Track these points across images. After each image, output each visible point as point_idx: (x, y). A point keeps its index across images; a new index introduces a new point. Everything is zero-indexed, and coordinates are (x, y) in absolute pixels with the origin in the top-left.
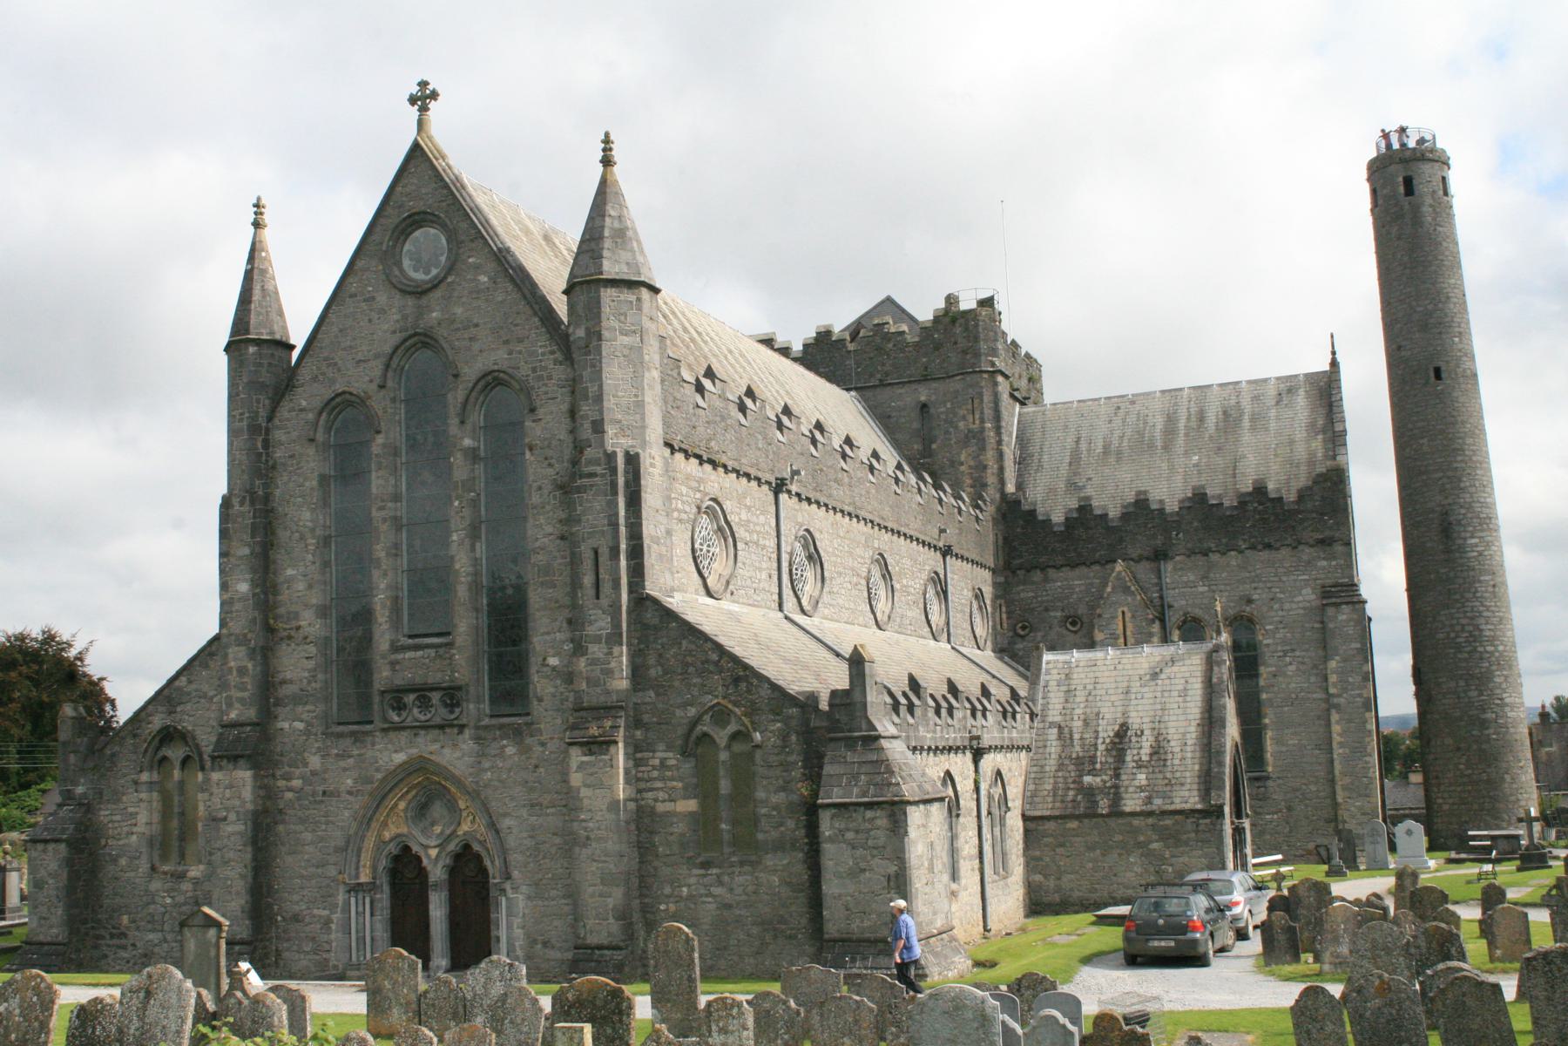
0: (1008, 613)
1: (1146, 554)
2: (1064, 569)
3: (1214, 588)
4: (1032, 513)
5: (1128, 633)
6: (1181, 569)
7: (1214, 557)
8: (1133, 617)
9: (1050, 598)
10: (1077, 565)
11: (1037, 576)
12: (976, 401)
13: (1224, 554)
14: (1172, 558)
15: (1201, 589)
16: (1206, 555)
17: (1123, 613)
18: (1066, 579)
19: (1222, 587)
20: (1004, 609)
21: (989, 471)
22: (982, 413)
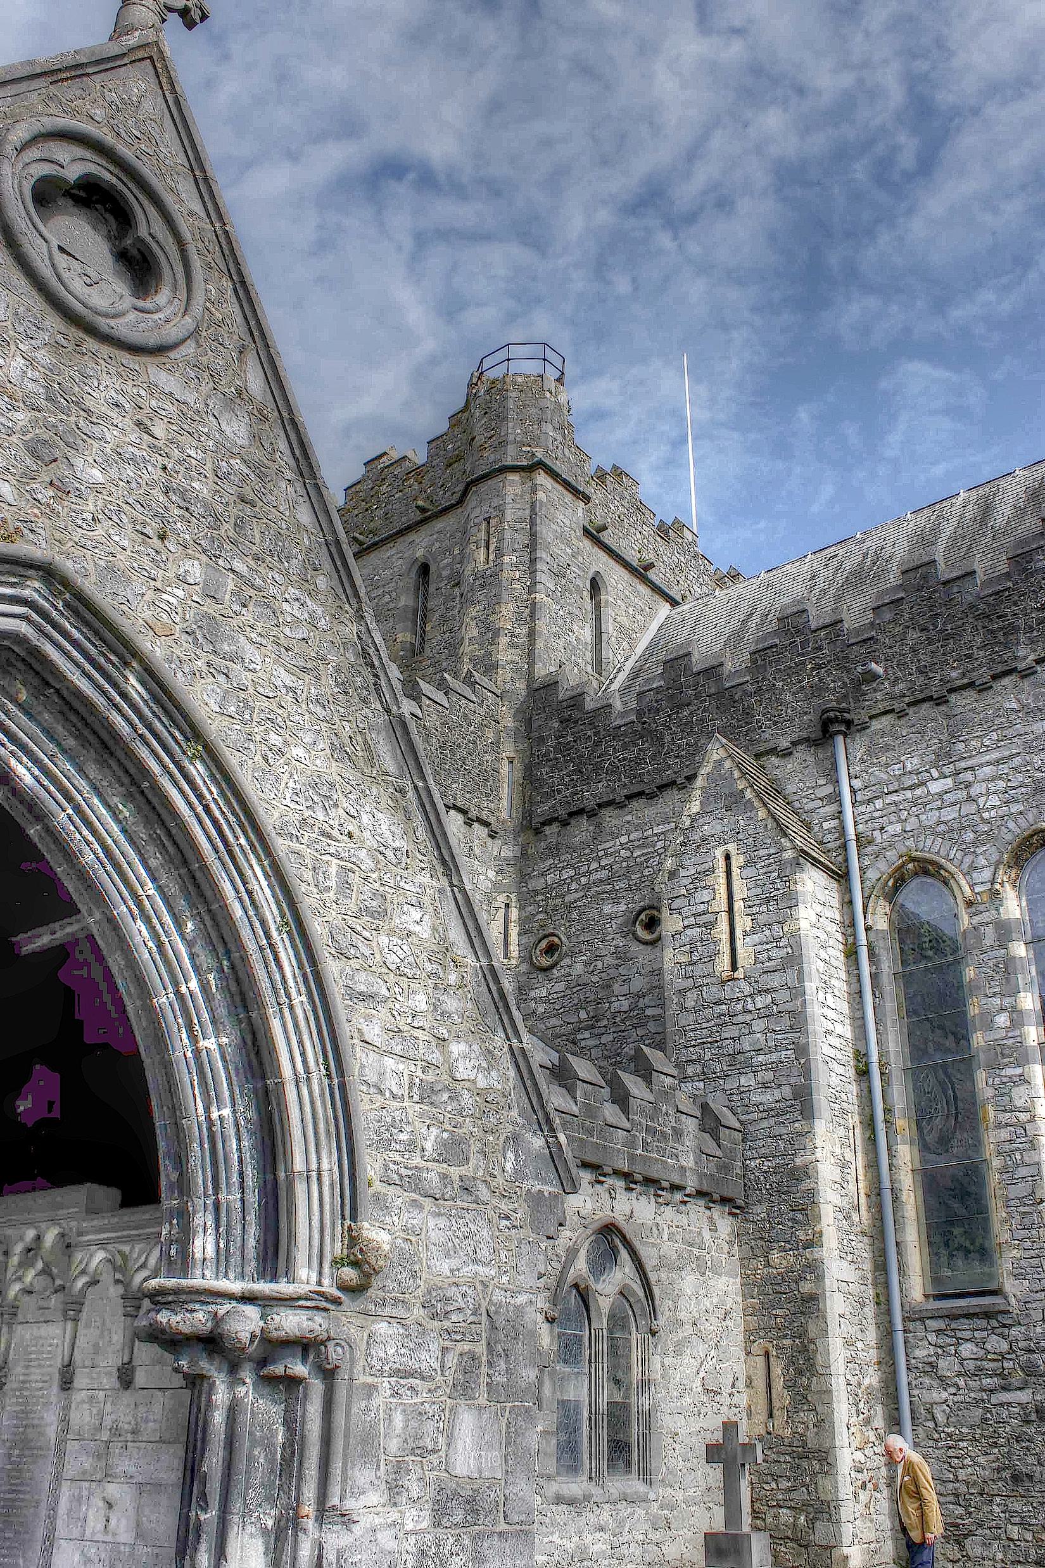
0: (521, 921)
1: (804, 734)
2: (635, 804)
3: (968, 776)
4: (577, 700)
5: (739, 906)
6: (887, 748)
7: (963, 702)
8: (749, 863)
9: (604, 874)
10: (662, 787)
11: (581, 831)
12: (493, 522)
13: (984, 688)
14: (864, 727)
15: (935, 787)
16: (941, 701)
17: (728, 857)
18: (638, 828)
19: (988, 770)
20: (514, 914)
21: (504, 641)
22: (501, 540)
